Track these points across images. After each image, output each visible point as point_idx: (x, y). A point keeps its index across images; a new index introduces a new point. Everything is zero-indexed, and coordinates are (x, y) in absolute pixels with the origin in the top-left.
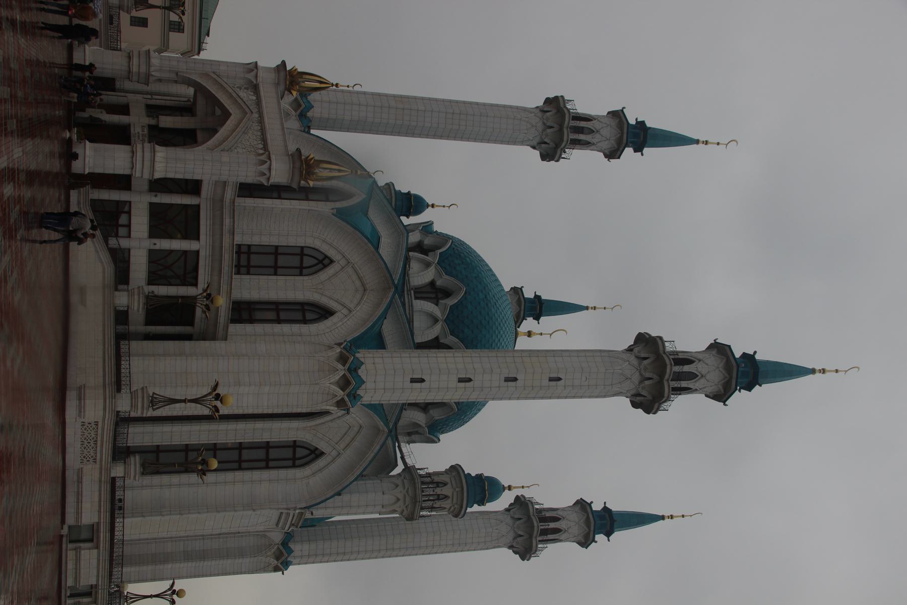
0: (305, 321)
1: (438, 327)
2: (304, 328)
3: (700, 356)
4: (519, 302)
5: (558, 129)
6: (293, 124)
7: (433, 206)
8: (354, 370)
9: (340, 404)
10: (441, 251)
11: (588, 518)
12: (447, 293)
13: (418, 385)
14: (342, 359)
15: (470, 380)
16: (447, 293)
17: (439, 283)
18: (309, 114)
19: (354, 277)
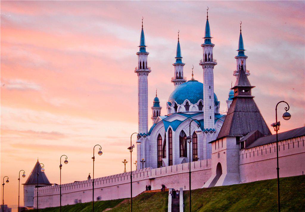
0: (197, 137)
1: (195, 105)
2: (198, 138)
3: (205, 53)
4: (178, 65)
5: (143, 69)
6: (149, 137)
7: (156, 95)
8: (209, 131)
9: (215, 133)
10: (177, 104)
11: (240, 58)
12: (187, 103)
13: (211, 118)
14: (206, 133)
15: (210, 106)
16: (187, 103)
17: (185, 105)
18: (146, 133)
19: (186, 127)
